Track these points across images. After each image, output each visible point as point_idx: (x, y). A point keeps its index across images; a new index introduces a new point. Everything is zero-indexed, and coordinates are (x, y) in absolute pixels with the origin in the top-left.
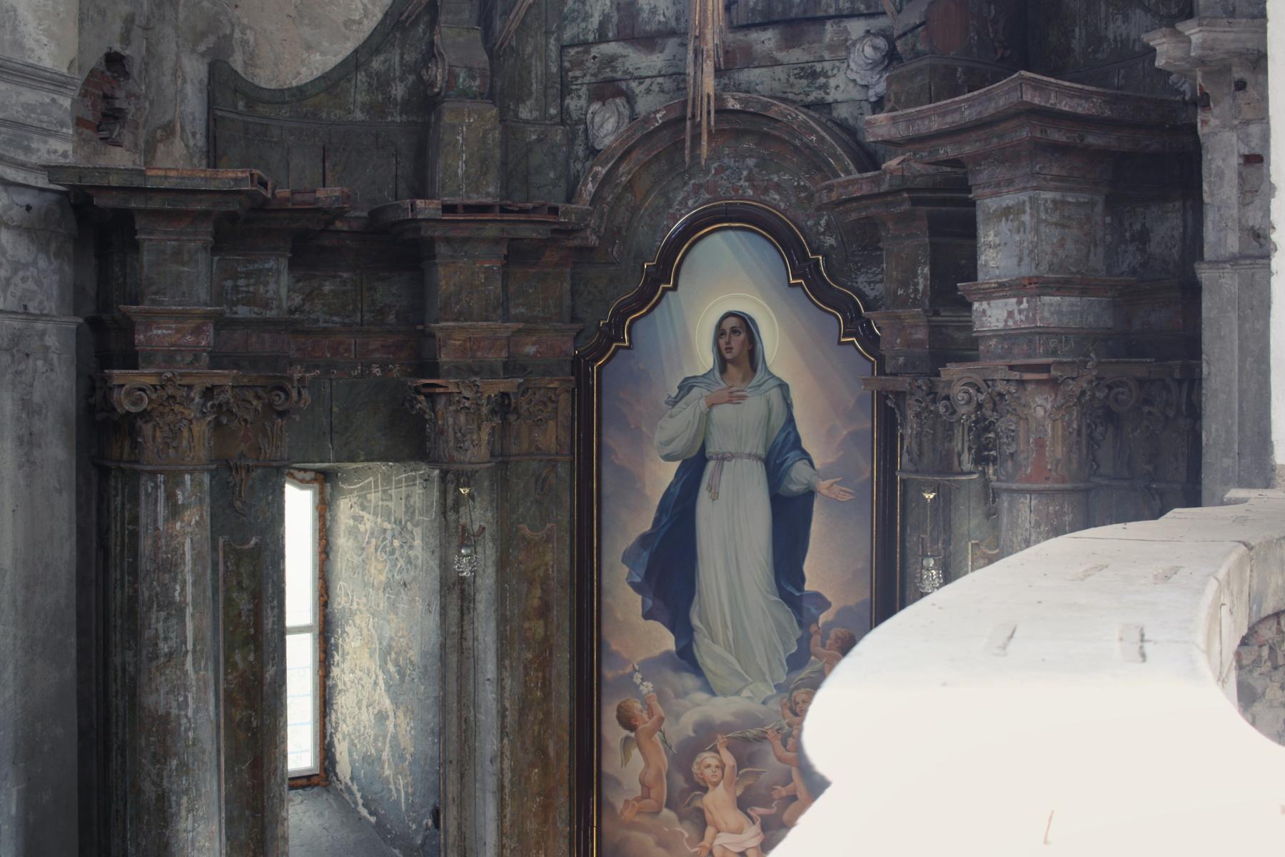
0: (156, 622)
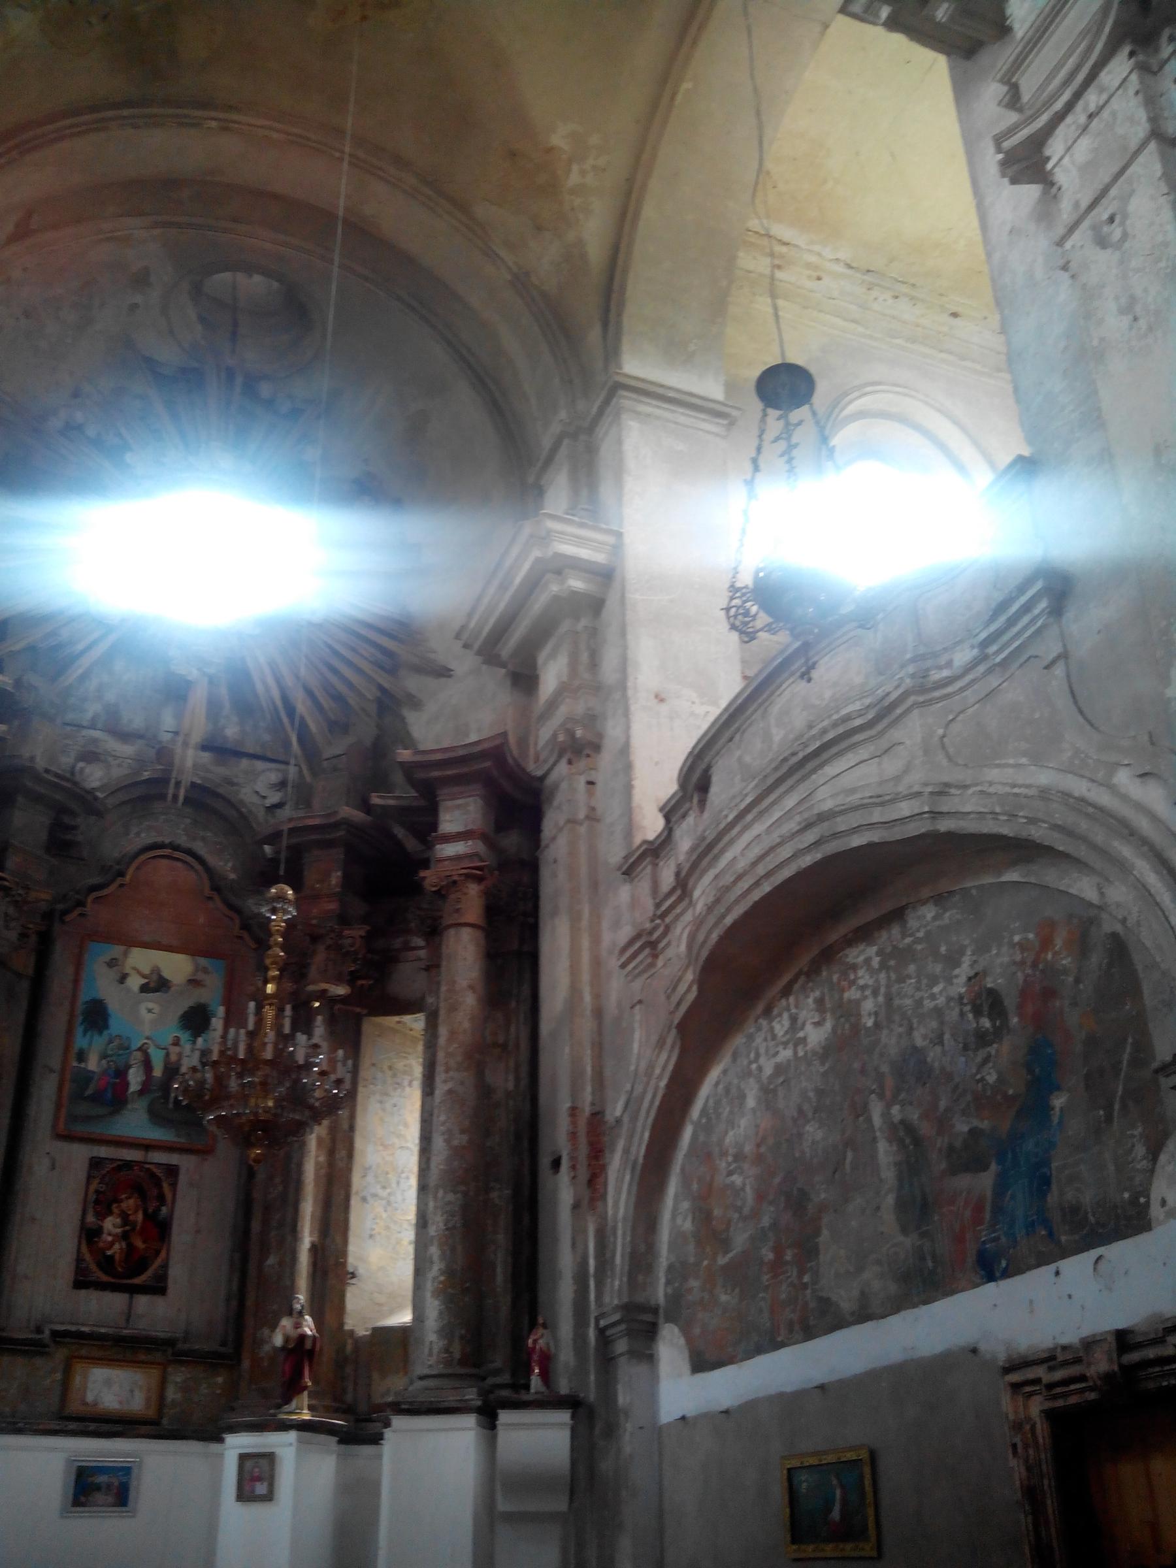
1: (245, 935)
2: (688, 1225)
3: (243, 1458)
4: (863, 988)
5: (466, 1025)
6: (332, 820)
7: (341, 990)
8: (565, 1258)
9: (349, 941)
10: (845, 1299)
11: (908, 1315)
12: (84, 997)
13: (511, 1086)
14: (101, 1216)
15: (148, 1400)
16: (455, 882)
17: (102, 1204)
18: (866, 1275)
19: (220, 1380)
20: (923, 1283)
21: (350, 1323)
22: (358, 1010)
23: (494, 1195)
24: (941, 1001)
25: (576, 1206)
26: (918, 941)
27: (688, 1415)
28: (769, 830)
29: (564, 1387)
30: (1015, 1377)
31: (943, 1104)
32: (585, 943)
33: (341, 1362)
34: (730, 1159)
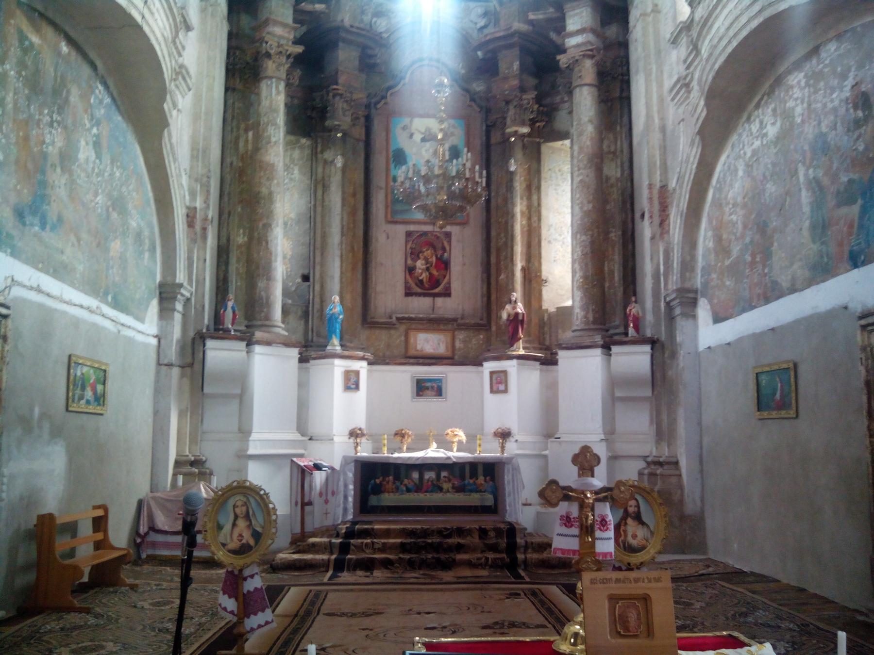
0: (271, 130)
1: (473, 104)
2: (711, 245)
3: (492, 373)
4: (796, 99)
5: (588, 143)
6: (510, 32)
7: (525, 130)
8: (647, 267)
9: (525, 102)
10: (784, 281)
11: (814, 288)
12: (392, 148)
13: (619, 175)
14: (415, 260)
15: (447, 347)
16: (577, 60)
17: (415, 254)
18: (795, 266)
19: (481, 336)
20: (822, 271)
21: (545, 306)
22: (538, 140)
23: (612, 235)
24: (836, 103)
25: (653, 238)
26: (826, 66)
27: (712, 345)
28: (736, 7)
29: (649, 333)
30: (863, 322)
31: (835, 166)
32: (655, 89)
33: (542, 325)
34: (731, 206)
